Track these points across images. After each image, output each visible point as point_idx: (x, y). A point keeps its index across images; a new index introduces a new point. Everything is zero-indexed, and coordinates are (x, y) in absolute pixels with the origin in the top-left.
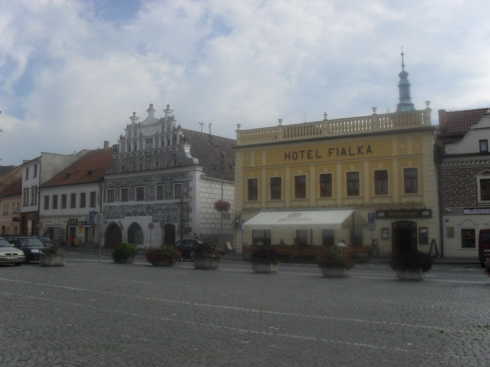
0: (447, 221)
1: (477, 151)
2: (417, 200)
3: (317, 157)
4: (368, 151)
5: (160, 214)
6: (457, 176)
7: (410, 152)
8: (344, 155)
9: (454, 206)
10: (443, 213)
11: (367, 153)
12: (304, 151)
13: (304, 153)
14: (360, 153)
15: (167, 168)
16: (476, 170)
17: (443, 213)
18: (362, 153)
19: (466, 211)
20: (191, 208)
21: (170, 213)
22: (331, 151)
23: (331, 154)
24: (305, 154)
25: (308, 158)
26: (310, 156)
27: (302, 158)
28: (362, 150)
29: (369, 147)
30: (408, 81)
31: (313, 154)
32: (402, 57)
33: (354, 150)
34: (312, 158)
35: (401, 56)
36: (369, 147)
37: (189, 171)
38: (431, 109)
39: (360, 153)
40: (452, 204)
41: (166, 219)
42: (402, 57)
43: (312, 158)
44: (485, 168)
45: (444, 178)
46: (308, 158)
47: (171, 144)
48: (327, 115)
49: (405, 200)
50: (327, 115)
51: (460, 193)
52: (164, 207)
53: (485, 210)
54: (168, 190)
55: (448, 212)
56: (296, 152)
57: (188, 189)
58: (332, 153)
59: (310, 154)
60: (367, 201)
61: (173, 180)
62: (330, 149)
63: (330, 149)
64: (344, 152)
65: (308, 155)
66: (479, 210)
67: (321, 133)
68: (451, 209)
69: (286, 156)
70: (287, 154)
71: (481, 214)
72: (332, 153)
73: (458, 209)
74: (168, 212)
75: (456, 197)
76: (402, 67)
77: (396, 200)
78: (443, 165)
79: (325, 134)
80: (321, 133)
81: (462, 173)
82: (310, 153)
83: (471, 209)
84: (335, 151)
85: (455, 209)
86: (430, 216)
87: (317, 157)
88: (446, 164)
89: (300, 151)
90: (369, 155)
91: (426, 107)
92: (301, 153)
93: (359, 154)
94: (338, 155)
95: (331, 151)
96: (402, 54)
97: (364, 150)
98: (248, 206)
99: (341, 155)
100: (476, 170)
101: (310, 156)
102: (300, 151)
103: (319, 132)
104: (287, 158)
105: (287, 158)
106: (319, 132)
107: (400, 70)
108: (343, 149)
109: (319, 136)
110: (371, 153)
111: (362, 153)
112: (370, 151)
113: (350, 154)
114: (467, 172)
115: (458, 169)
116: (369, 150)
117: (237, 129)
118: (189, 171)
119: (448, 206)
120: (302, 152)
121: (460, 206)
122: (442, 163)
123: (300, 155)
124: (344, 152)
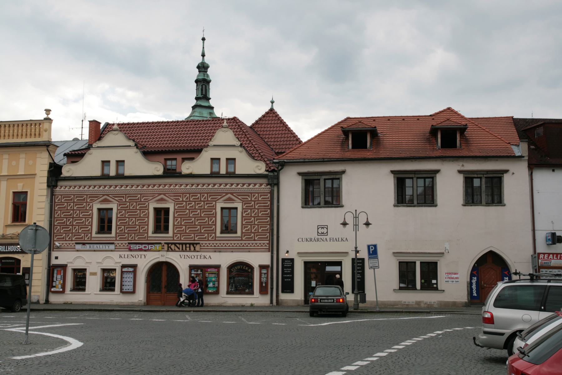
0: (57, 258)
1: (98, 173)
6: (72, 204)
9: (66, 240)
10: (53, 248)
16: (94, 197)
17: (53, 248)
19: (78, 247)
30: (208, 76)
32: (203, 43)
35: (202, 41)
38: (52, 120)
40: (63, 238)
42: (203, 43)
44: (104, 195)
45: (57, 205)
51: (74, 224)
53: (98, 245)
55: (59, 248)
66: (92, 245)
68: (59, 244)
71: (95, 251)
73: (69, 244)
75: (69, 229)
76: (202, 56)
78: (58, 189)
81: (78, 200)
83: (84, 244)
85: (66, 244)
88: (62, 188)
91: (45, 116)
96: (203, 39)
100: (94, 197)
107: (200, 60)
114: (84, 199)
115: (74, 195)
119: (58, 240)
121: (72, 241)
122: (56, 186)
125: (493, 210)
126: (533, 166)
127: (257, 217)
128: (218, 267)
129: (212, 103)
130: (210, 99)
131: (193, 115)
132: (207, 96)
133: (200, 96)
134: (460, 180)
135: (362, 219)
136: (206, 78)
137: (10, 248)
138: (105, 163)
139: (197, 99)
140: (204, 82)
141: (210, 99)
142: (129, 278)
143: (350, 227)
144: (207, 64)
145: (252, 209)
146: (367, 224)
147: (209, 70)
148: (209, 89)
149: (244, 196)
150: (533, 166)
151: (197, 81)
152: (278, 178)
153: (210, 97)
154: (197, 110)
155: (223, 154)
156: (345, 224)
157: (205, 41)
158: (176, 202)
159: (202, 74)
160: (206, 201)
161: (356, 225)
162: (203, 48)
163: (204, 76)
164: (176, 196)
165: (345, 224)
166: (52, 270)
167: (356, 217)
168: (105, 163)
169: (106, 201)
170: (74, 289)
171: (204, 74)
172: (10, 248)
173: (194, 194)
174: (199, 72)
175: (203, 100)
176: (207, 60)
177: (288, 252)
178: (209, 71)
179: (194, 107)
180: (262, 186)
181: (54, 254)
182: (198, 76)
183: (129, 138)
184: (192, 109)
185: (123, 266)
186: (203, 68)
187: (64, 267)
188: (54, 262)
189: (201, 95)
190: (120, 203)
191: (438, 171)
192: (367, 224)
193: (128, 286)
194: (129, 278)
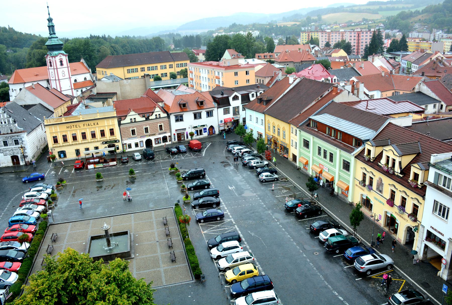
1: (130, 122)
2: (114, 138)
5: (8, 152)
7: (111, 124)
15: (8, 134)
16: (130, 127)
21: (14, 151)
24: (75, 126)
31: (78, 126)
33: (92, 124)
37: (20, 135)
41: (12, 154)
47: (7, 123)
49: (111, 138)
52: (10, 149)
54: (11, 142)
57: (22, 141)
60: (99, 140)
61: (13, 138)
64: (89, 125)
74: (13, 151)
86: (119, 142)
88: (122, 126)
90: (98, 126)
96: (48, 7)
97: (96, 124)
98: (55, 146)
100: (130, 127)
116: (97, 124)
123: (72, 127)
125: (212, 118)
127: (166, 126)
128: (160, 138)
133: (52, 33)
134: (206, 113)
138: (131, 119)
142: (142, 144)
143: (190, 128)
145: (165, 124)
149: (163, 122)
150: (218, 108)
151: (49, 27)
152: (170, 117)
155: (158, 113)
156: (189, 128)
158: (149, 126)
160: (156, 124)
164: (149, 124)
166: (123, 145)
168: (131, 119)
169: (133, 128)
170: (129, 148)
173: (153, 123)
174: (49, 22)
176: (51, 16)
178: (53, 21)
180: (167, 119)
181: (123, 141)
182: (49, 24)
183: (136, 113)
185: (140, 141)
186: (50, 20)
187: (126, 144)
188: (123, 143)
190: (137, 128)
191: (201, 112)
193: (142, 146)
194: (142, 144)
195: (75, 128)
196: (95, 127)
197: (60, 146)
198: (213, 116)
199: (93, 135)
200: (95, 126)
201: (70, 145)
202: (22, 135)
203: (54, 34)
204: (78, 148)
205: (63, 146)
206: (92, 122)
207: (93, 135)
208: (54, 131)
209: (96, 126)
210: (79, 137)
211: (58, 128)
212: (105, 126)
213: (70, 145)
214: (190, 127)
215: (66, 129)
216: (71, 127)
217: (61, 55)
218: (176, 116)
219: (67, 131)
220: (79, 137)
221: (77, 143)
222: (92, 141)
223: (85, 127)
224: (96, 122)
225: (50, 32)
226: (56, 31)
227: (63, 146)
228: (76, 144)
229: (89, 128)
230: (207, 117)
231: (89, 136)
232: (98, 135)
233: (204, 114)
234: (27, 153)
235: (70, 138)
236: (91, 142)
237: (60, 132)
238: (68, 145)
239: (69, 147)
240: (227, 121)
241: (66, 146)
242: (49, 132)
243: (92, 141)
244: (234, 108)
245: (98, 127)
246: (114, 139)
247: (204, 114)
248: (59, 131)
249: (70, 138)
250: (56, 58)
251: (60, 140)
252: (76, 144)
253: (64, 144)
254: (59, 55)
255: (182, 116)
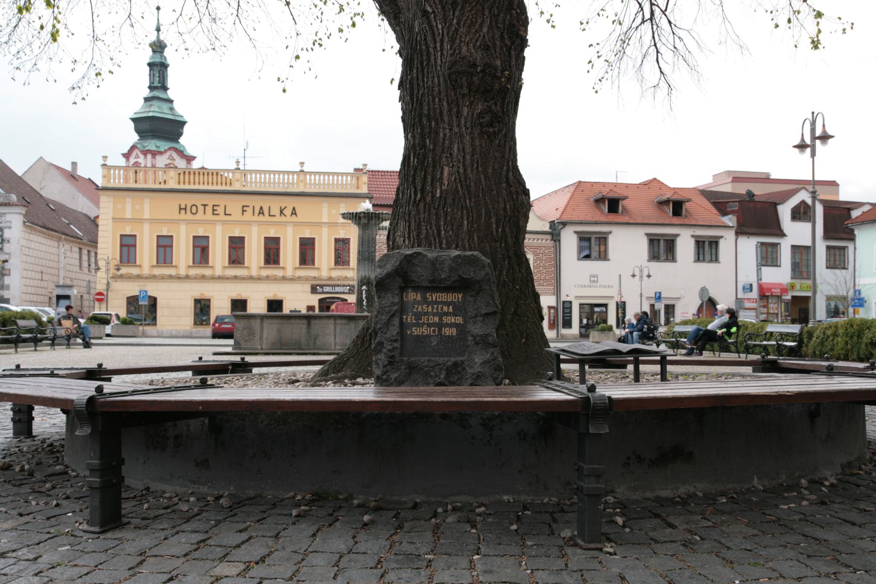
3: (225, 214)
4: (292, 214)
8: (261, 215)
11: (291, 216)
12: (207, 205)
13: (207, 207)
14: (282, 215)
18: (285, 216)
20: (9, 270)
22: (245, 209)
23: (245, 213)
24: (209, 209)
25: (213, 214)
26: (215, 212)
27: (205, 213)
28: (284, 212)
29: (294, 208)
31: (220, 210)
32: (158, 13)
33: (275, 211)
34: (218, 214)
35: (156, 11)
36: (294, 208)
37: (4, 214)
39: (282, 215)
42: (158, 13)
43: (218, 214)
46: (213, 214)
48: (239, 162)
49: (335, 274)
50: (239, 162)
56: (194, 205)
58: (246, 211)
59: (216, 210)
62: (243, 206)
63: (243, 206)
64: (261, 212)
65: (214, 210)
67: (231, 184)
69: (180, 209)
70: (183, 206)
72: (246, 211)
77: (324, 273)
79: (237, 187)
80: (231, 184)
82: (215, 208)
84: (249, 210)
87: (225, 214)
89: (202, 205)
92: (203, 207)
93: (281, 215)
94: (254, 215)
95: (245, 209)
96: (158, 8)
97: (288, 212)
99: (259, 215)
101: (215, 212)
102: (202, 205)
103: (228, 182)
104: (183, 212)
105: (183, 212)
106: (228, 182)
107: (153, 37)
108: (261, 208)
109: (228, 188)
110: (296, 216)
111: (285, 216)
112: (295, 214)
113: (270, 215)
116: (294, 212)
117: (103, 162)
118: (4, 214)
120: (205, 205)
123: (201, 209)
124: (261, 212)
125: (712, 266)
126: (739, 233)
127: (544, 267)
129: (171, 94)
130: (168, 89)
131: (152, 110)
132: (166, 85)
133: (156, 84)
134: (692, 242)
135: (645, 273)
136: (163, 61)
137: (337, 289)
139: (151, 88)
140: (161, 67)
141: (168, 89)
143: (637, 278)
144: (165, 43)
145: (541, 260)
146: (649, 276)
147: (166, 50)
148: (167, 76)
152: (559, 235)
153: (169, 87)
154: (155, 103)
156: (634, 276)
157: (160, 11)
159: (158, 55)
161: (641, 277)
162: (158, 20)
163: (161, 59)
165: (634, 276)
167: (641, 271)
171: (161, 56)
172: (337, 289)
174: (154, 51)
175: (160, 90)
176: (162, 38)
177: (567, 296)
178: (167, 53)
179: (147, 100)
182: (151, 58)
184: (143, 100)
186: (158, 47)
189: (159, 83)
191: (678, 235)
192: (649, 276)
195: (209, 215)
196: (284, 224)
197: (139, 277)
198: (717, 260)
199: (272, 253)
200: (283, 219)
201: (178, 278)
202: (8, 217)
203: (165, 88)
204: (207, 295)
205: (153, 278)
206: (275, 204)
207: (272, 253)
208: (128, 215)
209: (289, 218)
210: (219, 252)
211: (147, 207)
212: (319, 224)
213: (178, 278)
214: (637, 273)
215: (175, 215)
216: (194, 209)
217: (174, 155)
218: (584, 239)
219: (177, 222)
220: (219, 252)
221: (207, 272)
222: (265, 273)
223: (248, 216)
224: (289, 203)
225: (151, 82)
226: (171, 82)
227: (153, 278)
228: (203, 277)
229: (260, 223)
230: (695, 261)
231: (254, 253)
232: (290, 253)
233: (685, 246)
234: (8, 287)
235: (183, 253)
236: (259, 279)
237: (152, 221)
238: (171, 277)
239: (175, 286)
240: (770, 290)
241: (163, 278)
242: (111, 215)
243: (265, 273)
244: (796, 249)
245: (296, 224)
246: (346, 278)
247: (685, 246)
248: (147, 215)
249: (183, 253)
250: (158, 157)
251: (146, 252)
252: (203, 277)
253: (158, 271)
254: (168, 153)
255: (603, 239)
